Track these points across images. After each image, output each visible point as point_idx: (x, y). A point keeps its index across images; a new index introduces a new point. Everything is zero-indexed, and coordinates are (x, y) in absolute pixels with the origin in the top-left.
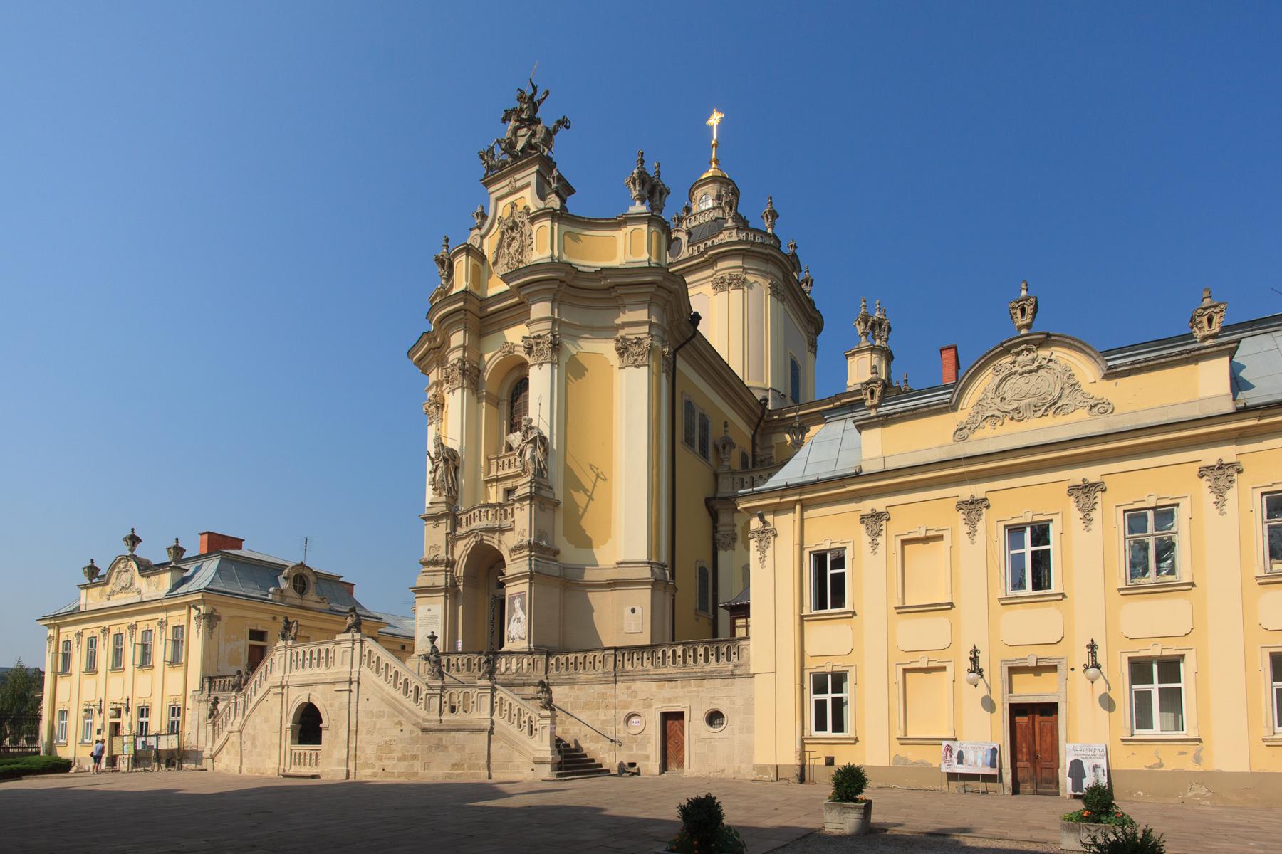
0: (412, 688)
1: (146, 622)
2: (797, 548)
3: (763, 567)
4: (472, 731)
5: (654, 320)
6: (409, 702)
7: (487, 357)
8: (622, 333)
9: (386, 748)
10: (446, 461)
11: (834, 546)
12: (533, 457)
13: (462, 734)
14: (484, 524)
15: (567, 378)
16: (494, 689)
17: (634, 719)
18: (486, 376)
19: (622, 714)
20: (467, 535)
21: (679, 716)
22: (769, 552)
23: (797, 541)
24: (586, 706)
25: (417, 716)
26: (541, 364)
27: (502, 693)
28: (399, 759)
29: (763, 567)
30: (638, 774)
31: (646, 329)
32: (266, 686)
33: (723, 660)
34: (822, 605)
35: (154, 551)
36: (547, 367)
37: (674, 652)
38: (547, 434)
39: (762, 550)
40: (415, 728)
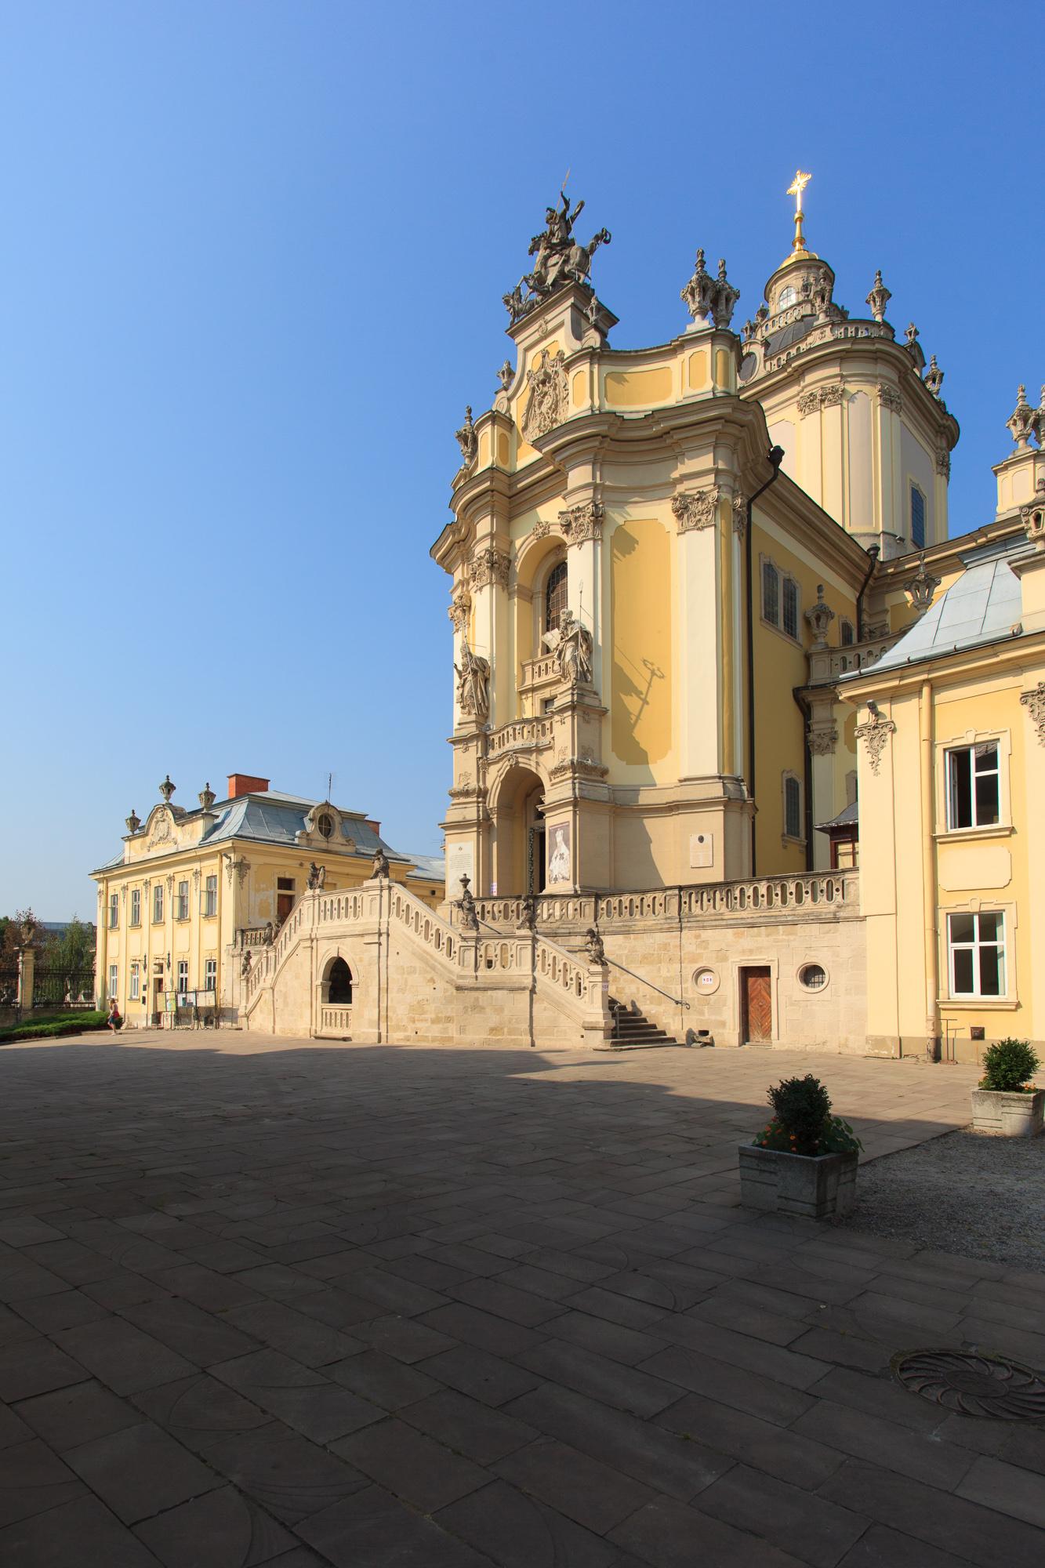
0: (444, 940)
1: (183, 873)
2: (925, 745)
3: (876, 773)
4: (512, 990)
5: (721, 466)
6: (441, 956)
7: (518, 543)
8: (680, 488)
9: (418, 1008)
10: (475, 672)
11: (980, 739)
12: (574, 658)
13: (500, 992)
14: (518, 744)
15: (613, 555)
16: (535, 940)
17: (704, 976)
18: (518, 566)
19: (690, 969)
20: (500, 758)
21: (765, 971)
22: (884, 754)
23: (925, 735)
24: (646, 959)
25: (450, 972)
26: (581, 543)
27: (544, 944)
28: (433, 1022)
29: (876, 773)
30: (711, 1044)
31: (711, 478)
32: (295, 939)
33: (822, 899)
34: (963, 820)
35: (188, 799)
36: (589, 545)
37: (756, 890)
38: (590, 628)
39: (874, 752)
40: (449, 986)
